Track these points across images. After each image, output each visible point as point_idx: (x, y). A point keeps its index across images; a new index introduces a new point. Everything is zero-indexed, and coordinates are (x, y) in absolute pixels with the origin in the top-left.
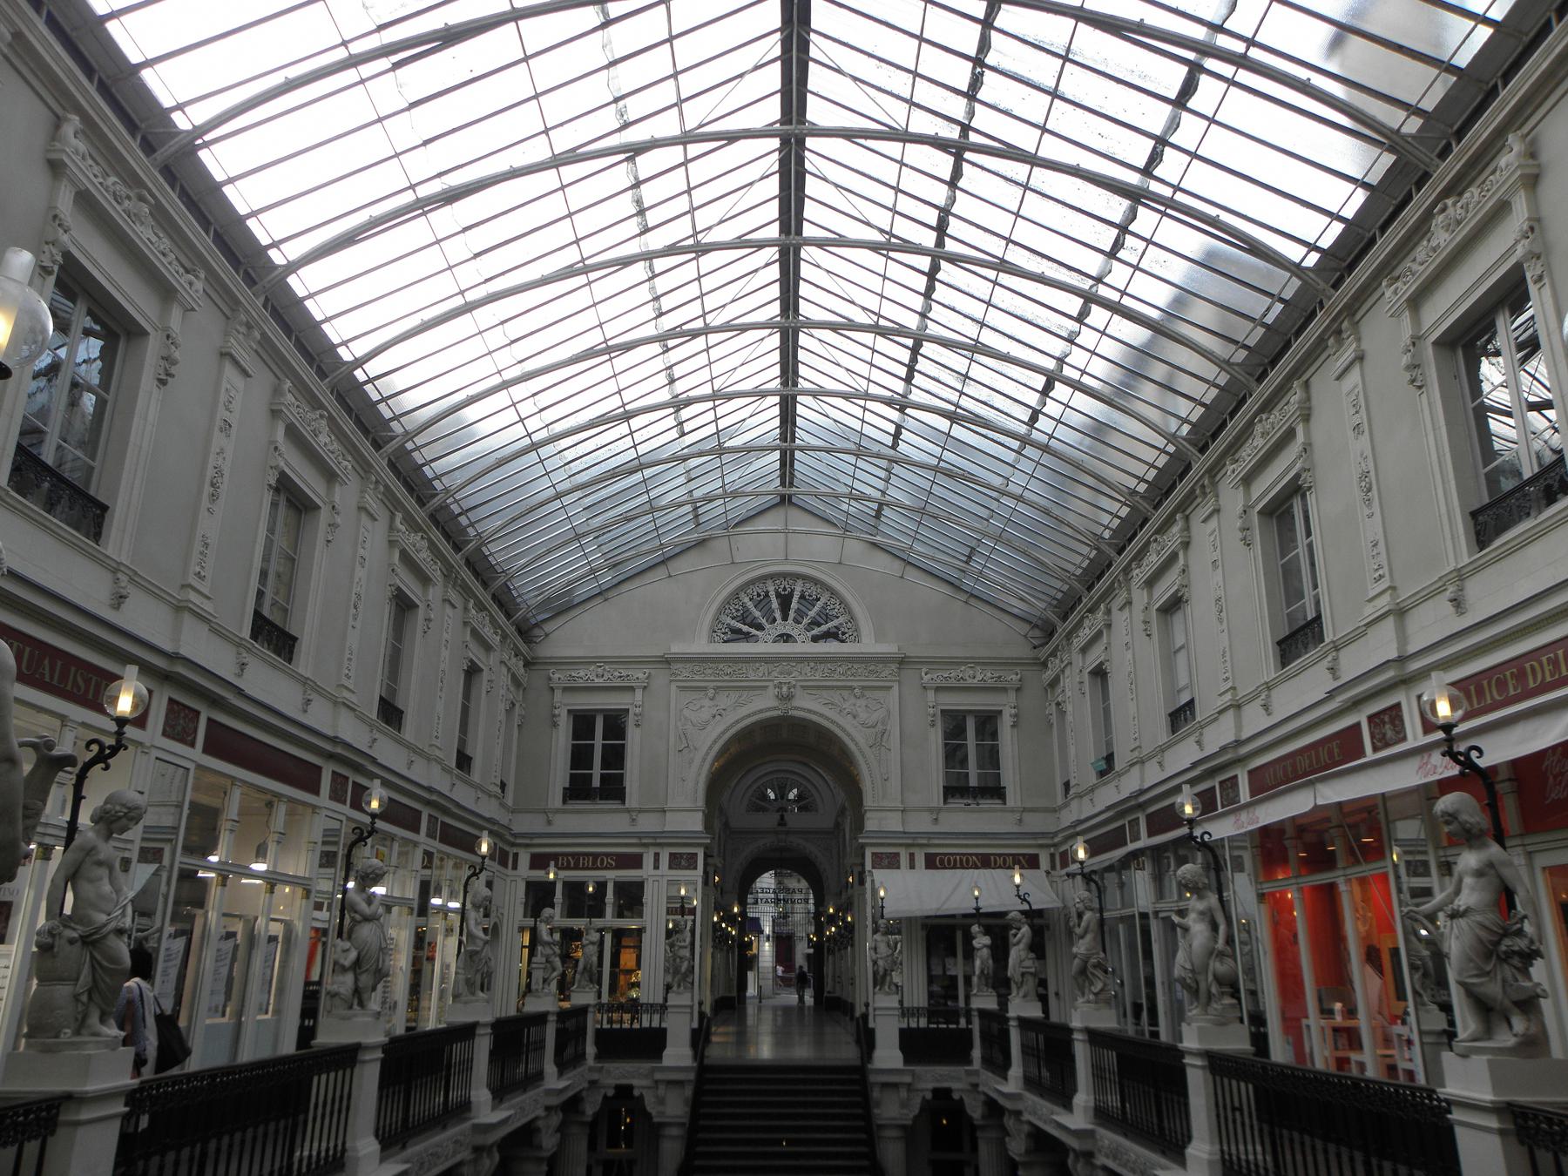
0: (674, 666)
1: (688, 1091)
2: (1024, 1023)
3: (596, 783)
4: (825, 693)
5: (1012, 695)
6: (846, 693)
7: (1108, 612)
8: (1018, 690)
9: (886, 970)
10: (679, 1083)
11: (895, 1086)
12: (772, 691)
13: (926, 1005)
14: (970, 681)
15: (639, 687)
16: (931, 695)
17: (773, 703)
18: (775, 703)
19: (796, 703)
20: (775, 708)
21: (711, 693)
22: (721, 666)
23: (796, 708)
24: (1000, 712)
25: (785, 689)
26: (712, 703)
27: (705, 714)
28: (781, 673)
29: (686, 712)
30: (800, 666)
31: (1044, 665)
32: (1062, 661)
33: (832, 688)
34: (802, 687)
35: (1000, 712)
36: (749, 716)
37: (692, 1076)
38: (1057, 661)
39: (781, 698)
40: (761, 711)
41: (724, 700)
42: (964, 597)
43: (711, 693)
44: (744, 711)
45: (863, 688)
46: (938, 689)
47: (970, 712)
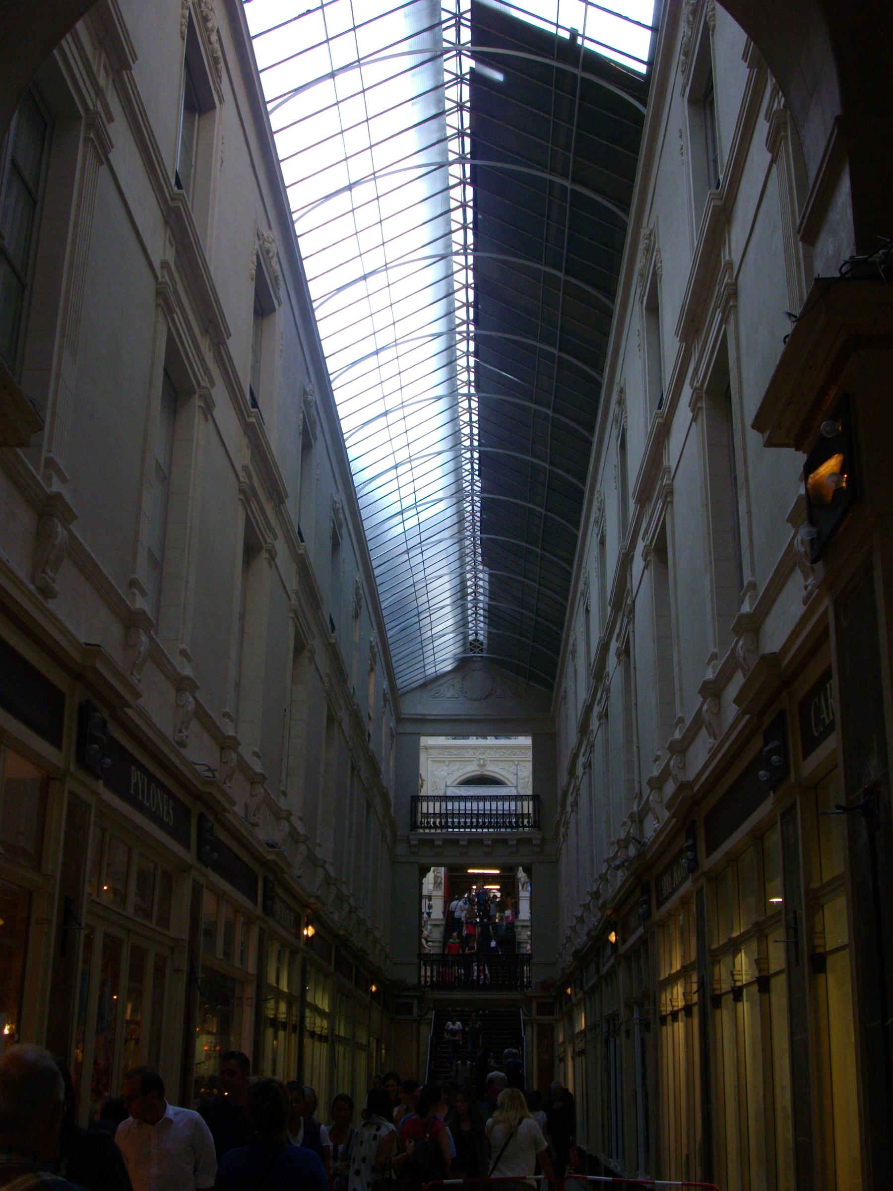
0: (430, 751)
1: (442, 928)
4: (500, 764)
6: (510, 763)
10: (438, 925)
12: (476, 763)
17: (477, 768)
18: (477, 768)
19: (488, 768)
20: (476, 771)
21: (447, 763)
22: (452, 751)
23: (487, 771)
25: (482, 761)
26: (447, 768)
27: (445, 774)
28: (480, 754)
29: (435, 772)
30: (488, 751)
33: (504, 761)
34: (490, 761)
36: (465, 774)
37: (443, 923)
39: (479, 765)
40: (470, 772)
41: (453, 767)
43: (447, 763)
44: (462, 772)
45: (519, 761)
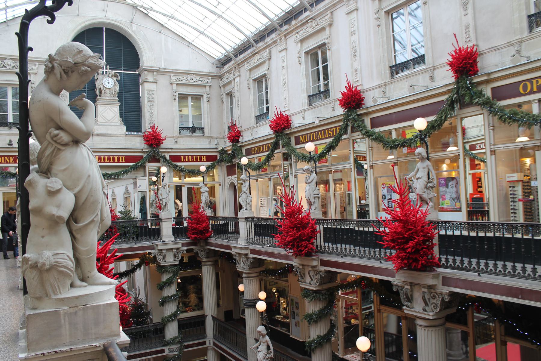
2: (248, 219)
3: (10, 120)
5: (208, 88)
7: (270, 53)
8: (210, 86)
9: (166, 203)
11: (172, 249)
13: (187, 216)
14: (191, 81)
15: (33, 73)
16: (174, 86)
24: (202, 96)
31: (220, 77)
32: (234, 75)
35: (202, 96)
38: (232, 75)
42: (188, 44)
46: (177, 84)
47: (189, 95)
